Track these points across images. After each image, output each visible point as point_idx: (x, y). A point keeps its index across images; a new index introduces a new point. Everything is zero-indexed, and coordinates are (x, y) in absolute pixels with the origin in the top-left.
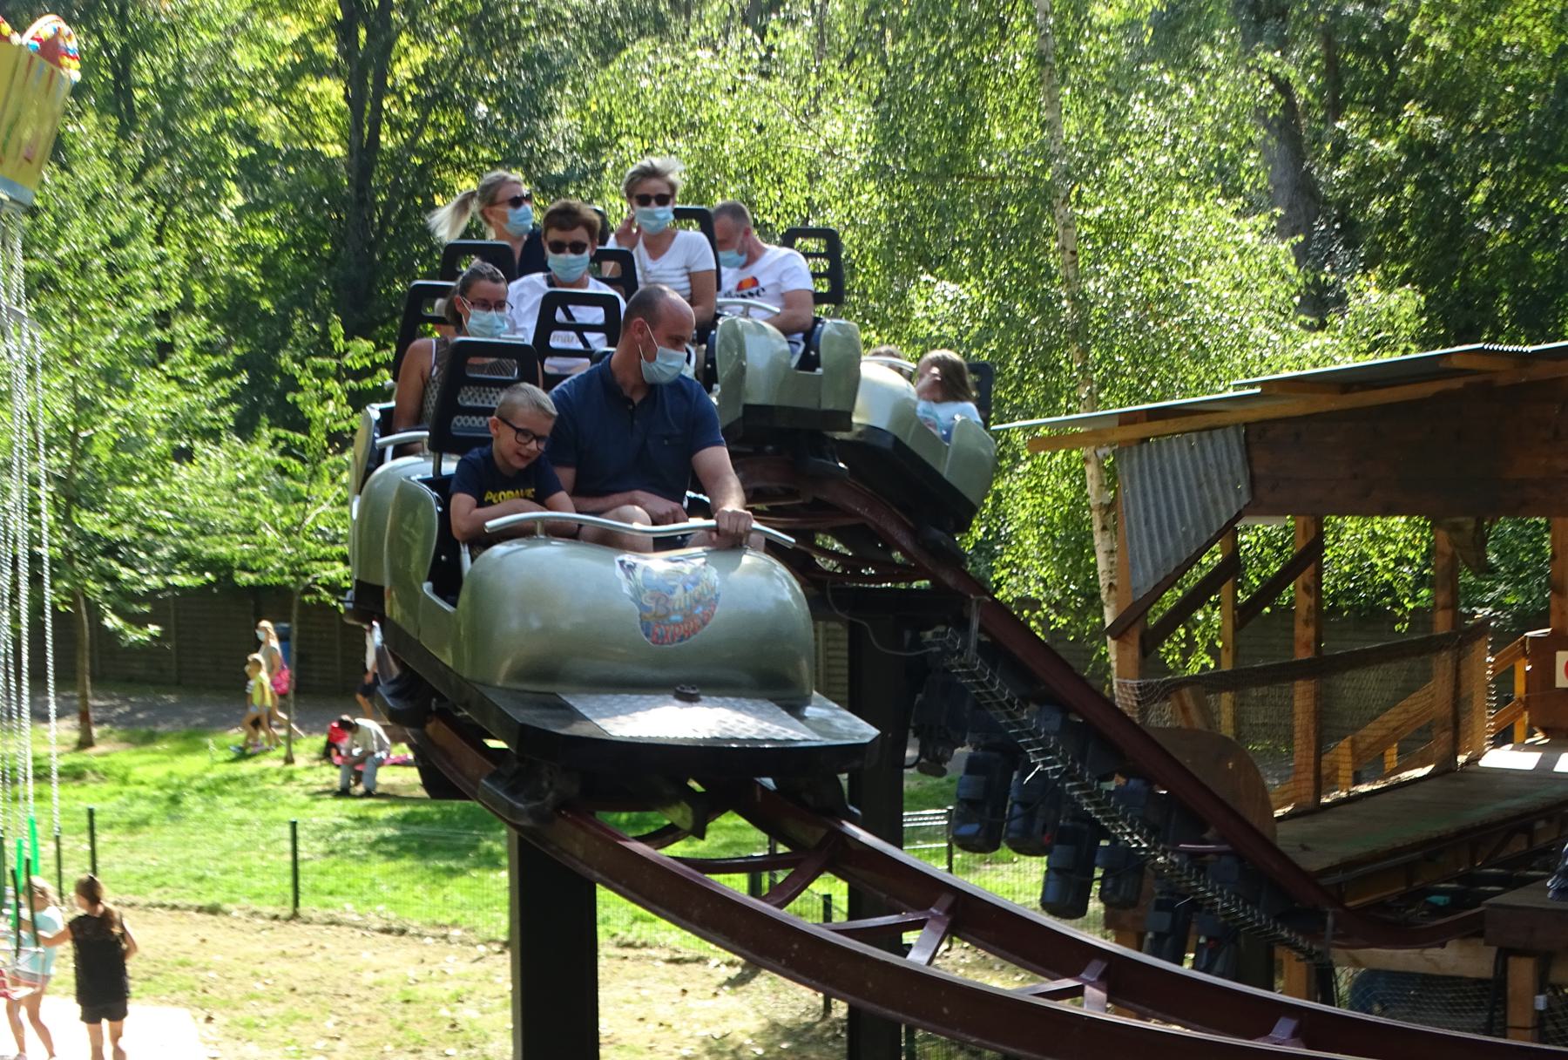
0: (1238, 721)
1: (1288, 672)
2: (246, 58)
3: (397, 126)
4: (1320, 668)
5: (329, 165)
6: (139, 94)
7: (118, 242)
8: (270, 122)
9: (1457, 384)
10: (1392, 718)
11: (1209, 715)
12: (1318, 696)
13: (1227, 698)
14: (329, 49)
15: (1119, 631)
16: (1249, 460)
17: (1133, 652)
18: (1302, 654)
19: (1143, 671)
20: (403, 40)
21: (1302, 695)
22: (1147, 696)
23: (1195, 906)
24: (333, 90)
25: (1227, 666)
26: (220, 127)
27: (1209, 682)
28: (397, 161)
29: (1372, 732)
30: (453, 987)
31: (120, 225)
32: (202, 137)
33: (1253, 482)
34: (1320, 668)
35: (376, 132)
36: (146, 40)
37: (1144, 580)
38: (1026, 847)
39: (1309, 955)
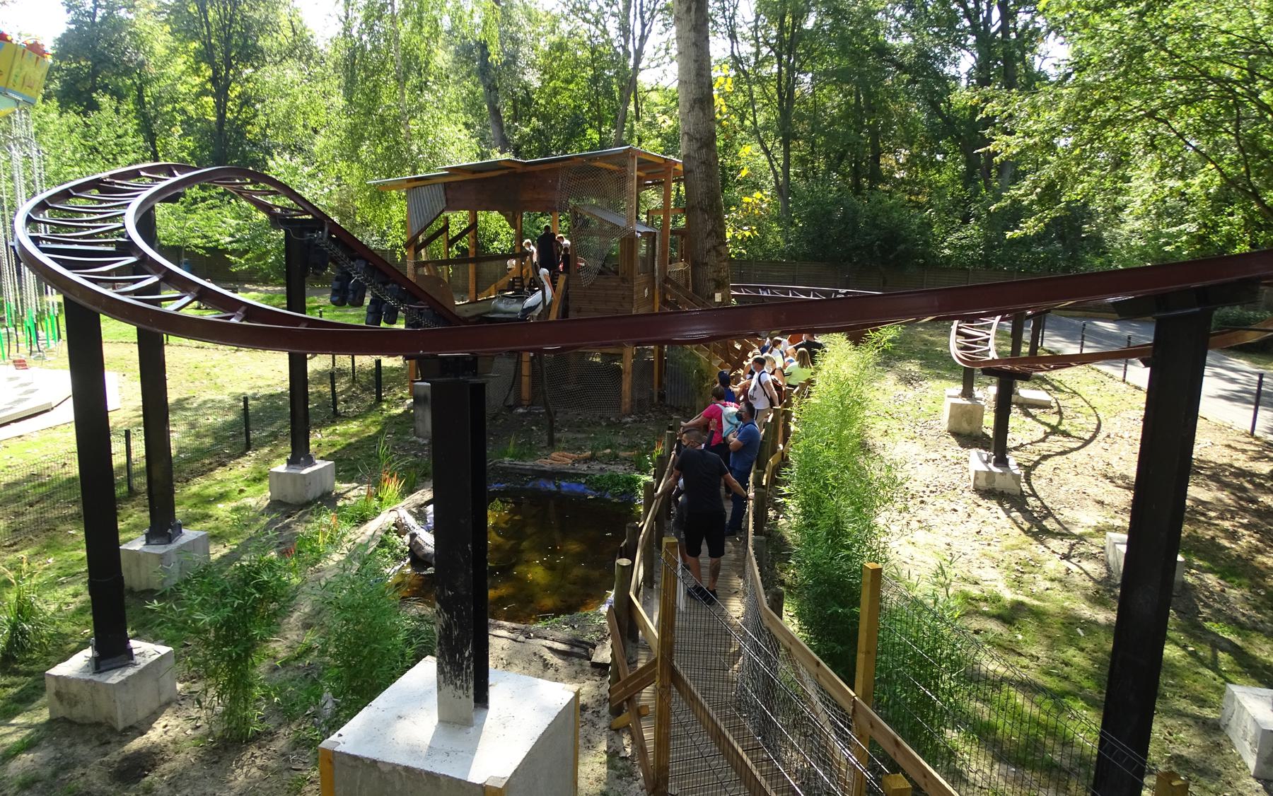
2: (182, 89)
3: (232, 111)
5: (210, 122)
6: (146, 99)
7: (119, 137)
8: (191, 108)
12: (476, 269)
14: (209, 86)
20: (233, 85)
24: (210, 101)
26: (174, 109)
28: (231, 122)
30: (213, 363)
31: (120, 132)
32: (167, 113)
35: (225, 112)
36: (148, 82)
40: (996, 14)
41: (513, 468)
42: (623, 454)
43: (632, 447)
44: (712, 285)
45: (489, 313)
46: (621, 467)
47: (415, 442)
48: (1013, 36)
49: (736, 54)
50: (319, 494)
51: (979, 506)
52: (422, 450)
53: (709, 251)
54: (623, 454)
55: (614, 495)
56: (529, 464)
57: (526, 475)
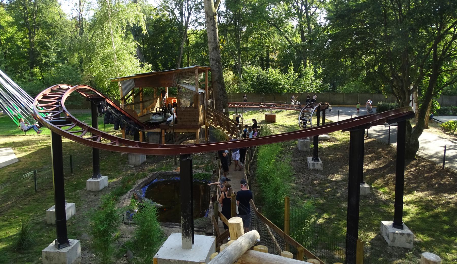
0: (135, 108)
1: (140, 102)
4: (143, 102)
9: (155, 74)
10: (150, 106)
11: (131, 107)
13: (133, 106)
15: (122, 100)
16: (135, 82)
17: (123, 101)
18: (141, 101)
19: (124, 104)
21: (141, 105)
22: (125, 106)
23: (130, 128)
25: (133, 102)
27: (132, 104)
29: (148, 108)
33: (135, 84)
34: (143, 102)
37: (124, 94)
38: (112, 123)
39: (142, 131)
40: (303, 7)
41: (166, 174)
42: (201, 166)
43: (202, 163)
44: (222, 106)
45: (149, 120)
46: (200, 171)
47: (129, 167)
48: (309, 14)
49: (221, 22)
50: (103, 188)
51: (311, 174)
52: (133, 170)
53: (220, 96)
54: (201, 166)
55: (200, 180)
56: (171, 172)
57: (170, 176)
